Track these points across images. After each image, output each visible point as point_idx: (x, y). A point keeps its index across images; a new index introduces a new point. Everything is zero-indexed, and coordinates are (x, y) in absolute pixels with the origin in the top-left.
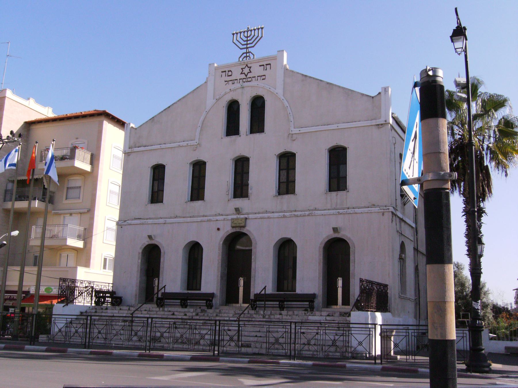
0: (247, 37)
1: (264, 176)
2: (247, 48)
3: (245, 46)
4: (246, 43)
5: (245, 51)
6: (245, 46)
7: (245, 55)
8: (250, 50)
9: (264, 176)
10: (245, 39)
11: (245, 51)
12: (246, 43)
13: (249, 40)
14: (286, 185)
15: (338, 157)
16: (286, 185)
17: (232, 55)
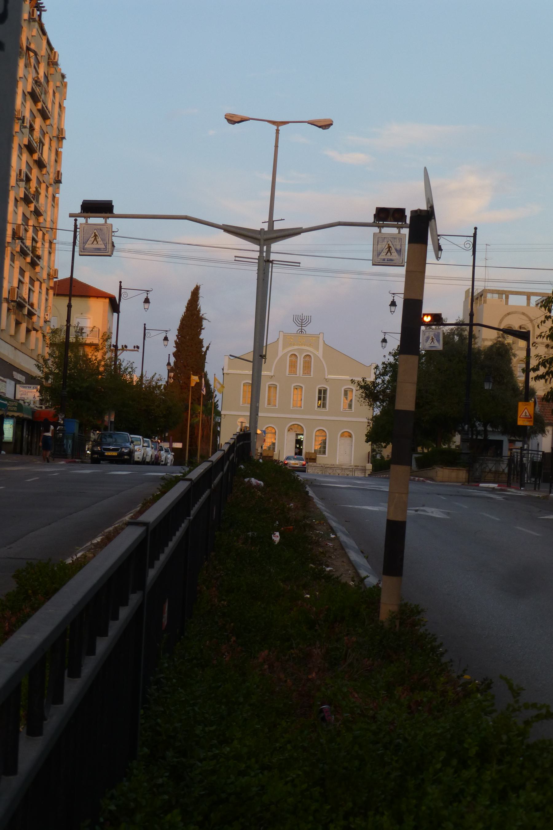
5: (300, 328)
8: (303, 328)
11: (300, 328)
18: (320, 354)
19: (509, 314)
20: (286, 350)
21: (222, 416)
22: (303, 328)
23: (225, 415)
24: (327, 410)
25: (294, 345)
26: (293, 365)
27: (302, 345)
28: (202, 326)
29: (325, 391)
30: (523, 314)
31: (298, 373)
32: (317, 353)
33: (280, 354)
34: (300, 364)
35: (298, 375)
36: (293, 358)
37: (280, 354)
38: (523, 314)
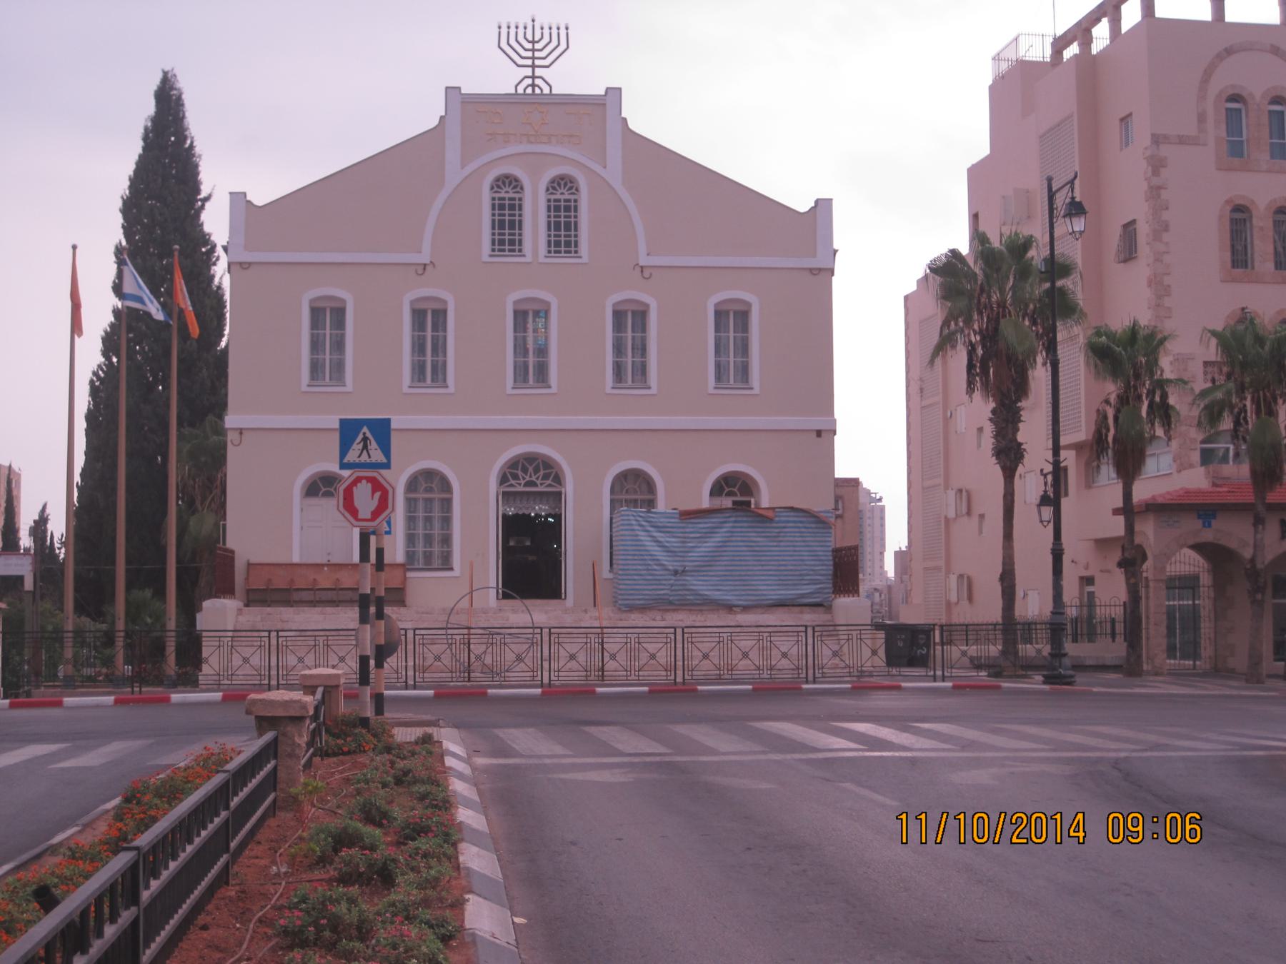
0: (533, 42)
1: (582, 344)
2: (533, 66)
3: (529, 62)
4: (530, 54)
5: (529, 72)
6: (529, 62)
7: (529, 81)
8: (538, 72)
9: (582, 344)
10: (529, 46)
11: (529, 72)
12: (530, 54)
14: (630, 365)
15: (733, 319)
16: (630, 365)
17: (502, 78)
18: (613, 173)
19: (1229, 51)
21: (231, 436)
22: (538, 72)
23: (241, 431)
24: (654, 391)
26: (507, 231)
28: (198, 191)
29: (641, 315)
30: (1275, 50)
32: (597, 168)
35: (528, 259)
37: (454, 174)
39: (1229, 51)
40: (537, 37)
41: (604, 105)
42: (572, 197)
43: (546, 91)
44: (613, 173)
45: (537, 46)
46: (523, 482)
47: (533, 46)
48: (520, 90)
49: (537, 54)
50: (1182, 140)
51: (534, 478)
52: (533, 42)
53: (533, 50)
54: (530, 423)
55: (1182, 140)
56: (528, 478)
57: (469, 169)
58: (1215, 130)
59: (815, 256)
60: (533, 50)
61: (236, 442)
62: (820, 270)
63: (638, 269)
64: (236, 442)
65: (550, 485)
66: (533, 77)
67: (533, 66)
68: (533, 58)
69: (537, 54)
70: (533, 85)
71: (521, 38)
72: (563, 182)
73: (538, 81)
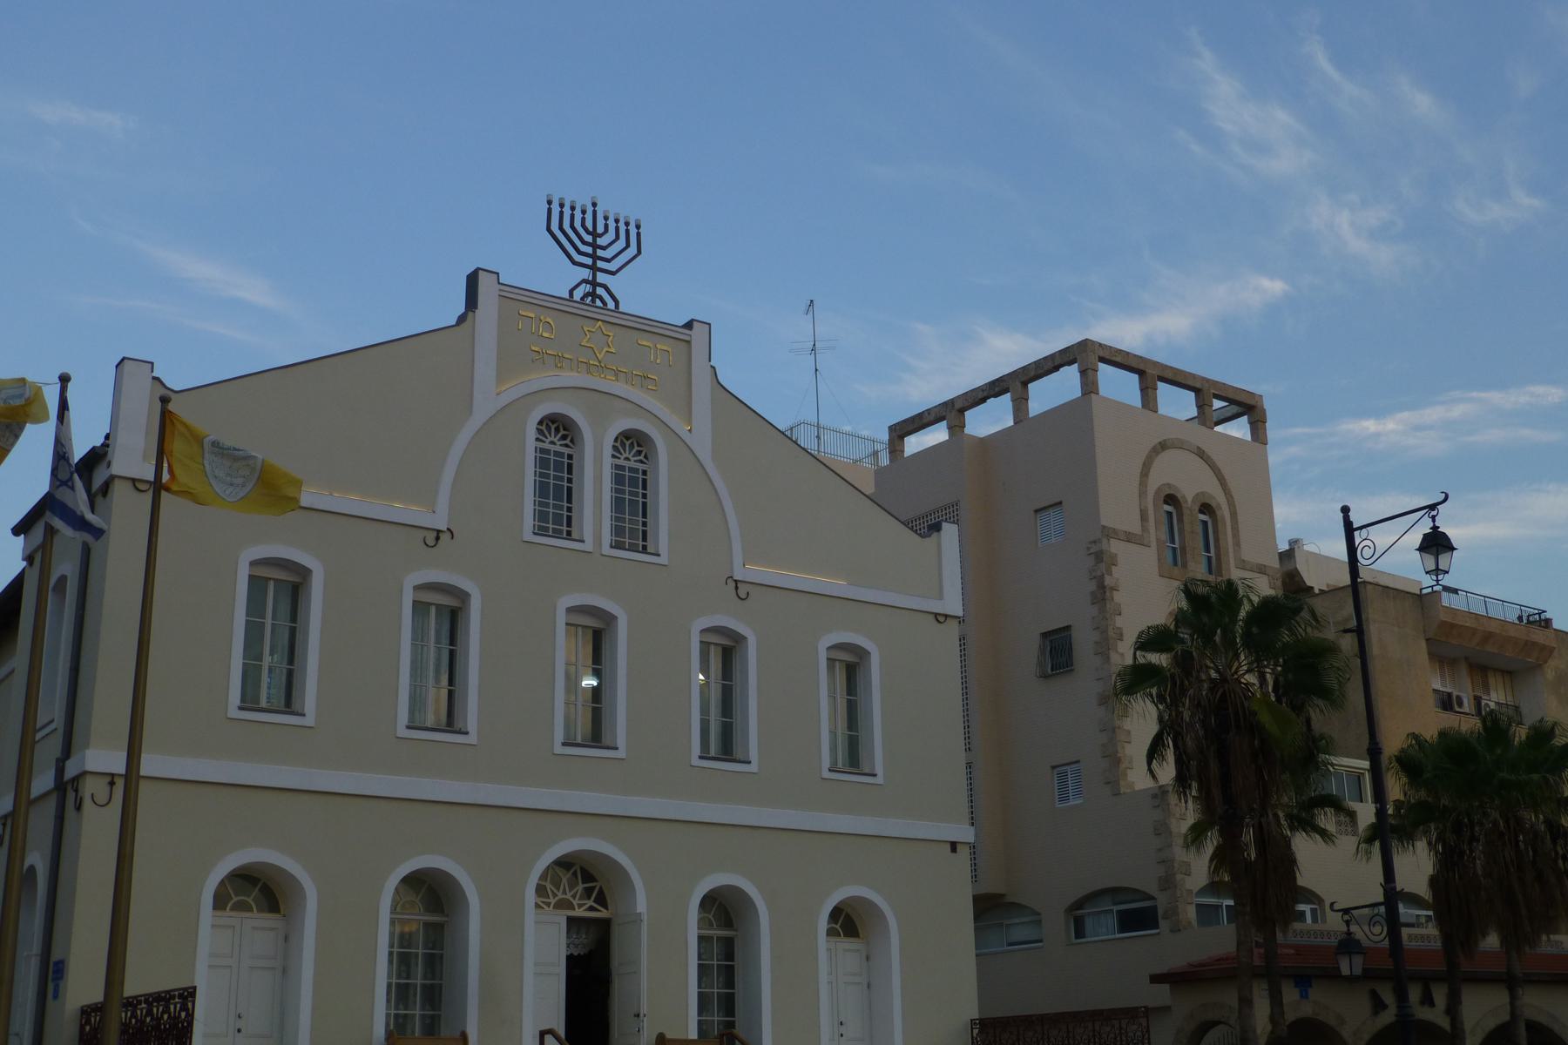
3: (589, 261)
4: (589, 250)
5: (586, 274)
6: (589, 261)
7: (589, 288)
8: (601, 278)
10: (589, 239)
11: (586, 274)
12: (589, 250)
13: (604, 248)
18: (701, 437)
19: (1163, 446)
20: (514, 390)
22: (601, 278)
25: (559, 361)
27: (602, 368)
30: (1201, 454)
31: (588, 535)
32: (682, 429)
33: (486, 402)
34: (598, 479)
35: (588, 546)
36: (555, 445)
37: (486, 402)
38: (1201, 454)
39: (1163, 446)
40: (600, 229)
41: (688, 342)
42: (641, 467)
43: (611, 305)
44: (701, 437)
45: (600, 241)
46: (553, 901)
47: (588, 237)
48: (578, 294)
49: (600, 253)
50: (1129, 538)
51: (568, 896)
52: (594, 234)
53: (595, 246)
54: (589, 805)
55: (1129, 538)
56: (560, 896)
57: (505, 399)
58: (1157, 532)
59: (940, 597)
60: (595, 246)
61: (102, 799)
62: (946, 616)
63: (732, 584)
64: (102, 799)
65: (591, 909)
66: (594, 284)
67: (594, 269)
68: (594, 257)
69: (600, 253)
70: (593, 295)
71: (578, 224)
72: (633, 441)
73: (600, 291)
